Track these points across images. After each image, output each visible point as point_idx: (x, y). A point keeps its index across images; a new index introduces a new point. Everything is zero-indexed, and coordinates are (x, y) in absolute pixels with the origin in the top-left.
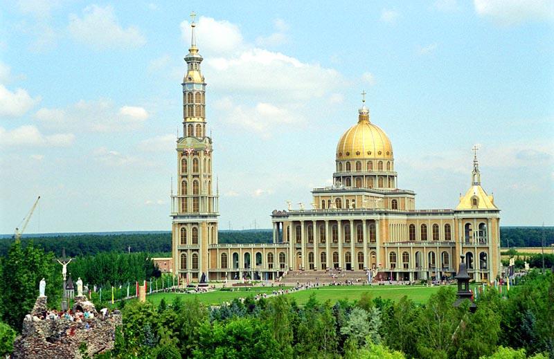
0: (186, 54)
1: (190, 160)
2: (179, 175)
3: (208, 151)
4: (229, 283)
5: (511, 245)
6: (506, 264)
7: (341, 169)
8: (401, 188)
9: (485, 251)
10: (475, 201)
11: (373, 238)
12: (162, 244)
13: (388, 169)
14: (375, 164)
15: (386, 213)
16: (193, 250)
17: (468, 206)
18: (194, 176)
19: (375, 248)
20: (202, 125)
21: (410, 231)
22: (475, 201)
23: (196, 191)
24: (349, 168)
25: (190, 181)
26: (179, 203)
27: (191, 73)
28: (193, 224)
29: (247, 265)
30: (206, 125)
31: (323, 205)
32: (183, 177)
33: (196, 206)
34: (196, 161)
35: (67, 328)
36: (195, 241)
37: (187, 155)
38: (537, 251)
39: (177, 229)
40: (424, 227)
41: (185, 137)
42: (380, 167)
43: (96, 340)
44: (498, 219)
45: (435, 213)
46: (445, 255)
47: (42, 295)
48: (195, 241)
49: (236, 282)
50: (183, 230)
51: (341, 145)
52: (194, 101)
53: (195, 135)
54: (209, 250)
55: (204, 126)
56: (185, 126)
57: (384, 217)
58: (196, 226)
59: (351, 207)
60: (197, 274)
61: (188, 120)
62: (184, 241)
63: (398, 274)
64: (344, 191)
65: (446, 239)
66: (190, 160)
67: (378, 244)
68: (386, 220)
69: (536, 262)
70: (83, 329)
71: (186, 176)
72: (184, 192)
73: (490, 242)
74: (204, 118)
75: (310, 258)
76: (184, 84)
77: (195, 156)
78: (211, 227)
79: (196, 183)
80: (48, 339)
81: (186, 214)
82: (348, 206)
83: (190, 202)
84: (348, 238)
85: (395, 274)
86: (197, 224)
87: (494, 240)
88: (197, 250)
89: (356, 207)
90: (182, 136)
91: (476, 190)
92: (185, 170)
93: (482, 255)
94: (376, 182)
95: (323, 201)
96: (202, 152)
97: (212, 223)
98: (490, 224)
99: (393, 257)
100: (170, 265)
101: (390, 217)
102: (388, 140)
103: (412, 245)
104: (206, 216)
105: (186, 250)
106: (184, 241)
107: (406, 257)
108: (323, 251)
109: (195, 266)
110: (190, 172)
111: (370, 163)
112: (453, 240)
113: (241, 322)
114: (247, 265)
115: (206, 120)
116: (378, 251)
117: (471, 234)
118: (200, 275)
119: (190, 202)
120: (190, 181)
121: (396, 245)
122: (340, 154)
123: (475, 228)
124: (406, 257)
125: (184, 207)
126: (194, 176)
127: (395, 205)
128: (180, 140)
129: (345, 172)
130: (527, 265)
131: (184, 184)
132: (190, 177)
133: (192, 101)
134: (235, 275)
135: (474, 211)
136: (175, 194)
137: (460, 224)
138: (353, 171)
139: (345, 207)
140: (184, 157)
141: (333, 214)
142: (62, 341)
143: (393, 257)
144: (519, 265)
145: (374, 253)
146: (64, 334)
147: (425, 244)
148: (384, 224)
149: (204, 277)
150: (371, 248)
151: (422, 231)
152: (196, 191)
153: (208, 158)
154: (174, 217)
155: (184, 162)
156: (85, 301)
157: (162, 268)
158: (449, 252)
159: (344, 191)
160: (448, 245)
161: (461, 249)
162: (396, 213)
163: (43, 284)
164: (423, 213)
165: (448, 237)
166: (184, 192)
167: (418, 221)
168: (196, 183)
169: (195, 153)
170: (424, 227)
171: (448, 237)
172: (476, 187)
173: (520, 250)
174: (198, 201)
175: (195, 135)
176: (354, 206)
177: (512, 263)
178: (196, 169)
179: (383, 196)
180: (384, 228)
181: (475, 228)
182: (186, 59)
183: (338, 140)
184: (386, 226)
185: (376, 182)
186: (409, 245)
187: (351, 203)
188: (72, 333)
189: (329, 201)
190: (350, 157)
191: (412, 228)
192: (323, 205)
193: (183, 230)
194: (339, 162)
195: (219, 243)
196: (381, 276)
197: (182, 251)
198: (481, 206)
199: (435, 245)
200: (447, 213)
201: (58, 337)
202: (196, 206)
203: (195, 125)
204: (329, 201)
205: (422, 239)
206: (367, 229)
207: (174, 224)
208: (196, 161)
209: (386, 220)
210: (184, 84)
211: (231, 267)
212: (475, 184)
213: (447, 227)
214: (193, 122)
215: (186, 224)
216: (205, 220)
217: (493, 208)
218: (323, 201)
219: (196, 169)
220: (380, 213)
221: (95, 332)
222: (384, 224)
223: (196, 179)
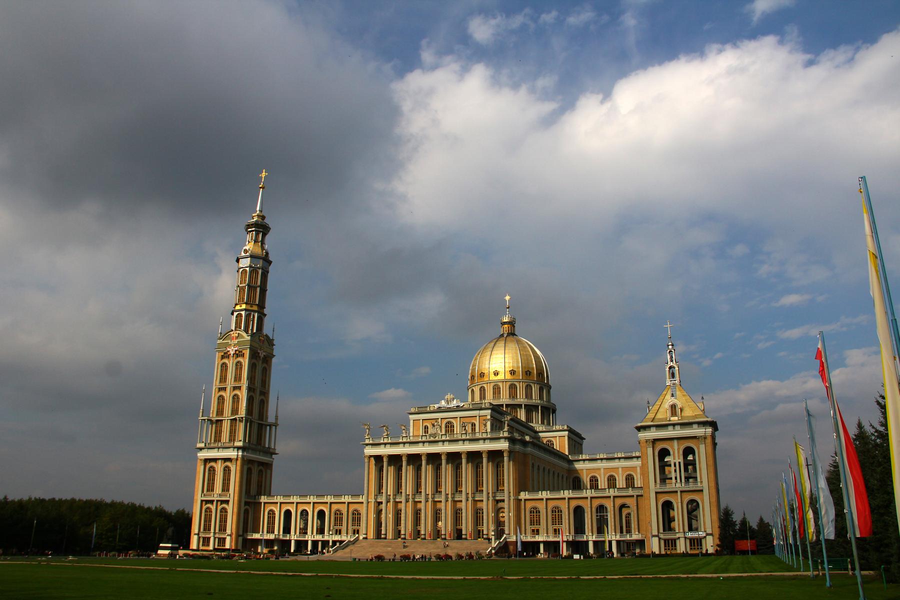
25: (228, 395)
36: (226, 488)
48: (226, 488)
62: (211, 488)
63: (542, 546)
72: (220, 412)
79: (236, 399)
97: (261, 464)
126: (235, 388)
140: (225, 360)
158: (631, 502)
161: (653, 495)
166: (220, 412)
193: (212, 470)
197: (207, 502)
214: (242, 310)
215: (215, 460)
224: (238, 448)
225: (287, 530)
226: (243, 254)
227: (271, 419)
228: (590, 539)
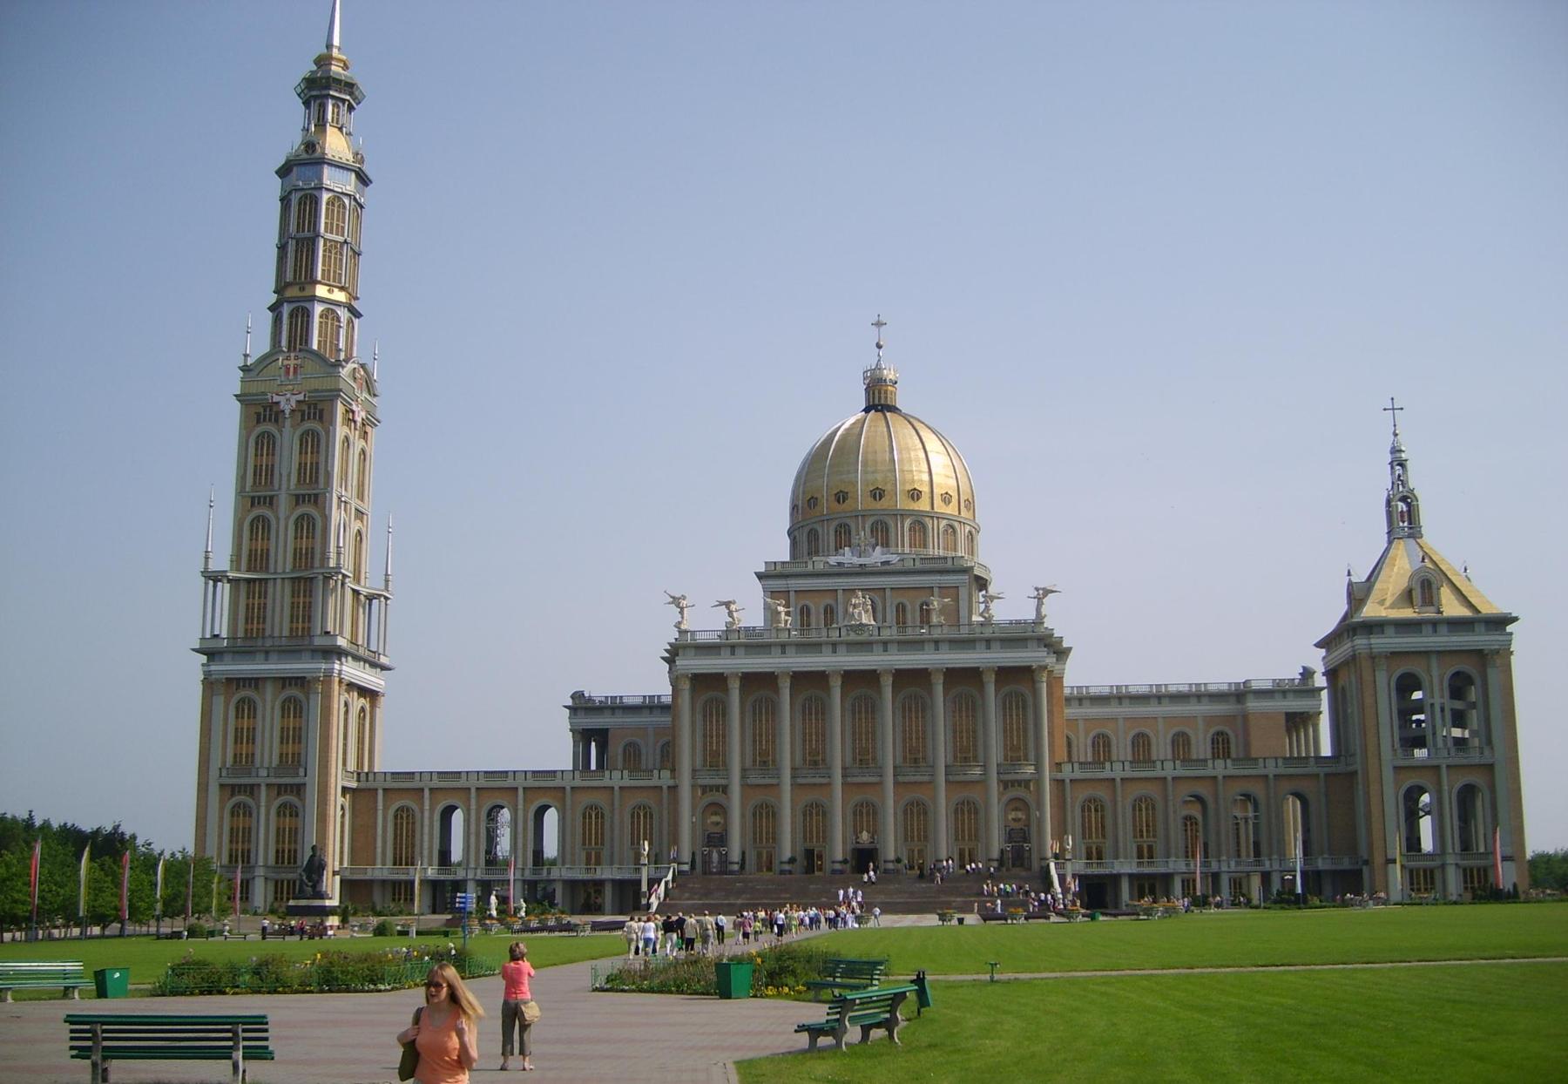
2: (241, 491)
16: (281, 789)
18: (299, 499)
28: (285, 681)
32: (255, 501)
39: (219, 702)
50: (246, 708)
54: (344, 789)
77: (308, 425)
78: (358, 703)
83: (280, 600)
86: (301, 682)
105: (251, 790)
119: (280, 600)
132: (283, 503)
137: (1381, 678)
141: (865, 646)
154: (212, 654)
174: (310, 593)
193: (246, 708)
207: (209, 684)
215: (255, 682)
226: (305, 156)
228: (1224, 868)
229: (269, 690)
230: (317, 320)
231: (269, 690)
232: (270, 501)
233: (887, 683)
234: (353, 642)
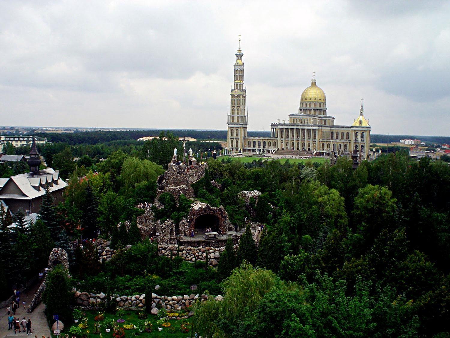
0: (236, 52)
1: (236, 99)
3: (244, 95)
4: (251, 154)
5: (374, 142)
6: (371, 150)
7: (302, 106)
8: (328, 115)
9: (363, 144)
10: (361, 122)
11: (315, 137)
12: (223, 135)
13: (323, 106)
14: (308, 104)
15: (321, 126)
16: (236, 139)
17: (358, 125)
18: (238, 107)
19: (315, 141)
20: (242, 84)
21: (331, 135)
22: (361, 122)
23: (238, 113)
24: (306, 106)
25: (236, 108)
26: (231, 119)
27: (238, 61)
28: (236, 127)
29: (259, 146)
30: (244, 84)
31: (294, 121)
32: (233, 107)
33: (238, 120)
34: (238, 100)
35: (186, 169)
36: (237, 135)
37: (235, 97)
38: (386, 145)
40: (337, 133)
41: (234, 89)
42: (320, 106)
43: (197, 175)
44: (370, 131)
45: (343, 127)
46: (346, 146)
47: (175, 155)
48: (237, 135)
49: (254, 153)
51: (302, 95)
52: (239, 73)
53: (239, 88)
55: (243, 85)
56: (234, 84)
57: (320, 128)
58: (238, 129)
59: (306, 123)
60: (238, 149)
61: (236, 82)
62: (232, 135)
64: (303, 116)
65: (347, 139)
66: (236, 99)
67: (317, 140)
68: (321, 129)
69: (384, 150)
70: (192, 169)
71: (239, 107)
72: (233, 113)
73: (366, 140)
74: (243, 81)
75: (287, 144)
76: (235, 66)
77: (238, 98)
78: (244, 129)
79: (238, 110)
80: (178, 173)
81: (233, 123)
82: (305, 123)
83: (236, 118)
84: (304, 136)
85: (323, 153)
86: (238, 127)
87: (367, 140)
88: (238, 139)
89: (308, 123)
90: (233, 89)
91: (361, 118)
92: (234, 104)
93: (362, 146)
94: (318, 112)
95: (294, 120)
96: (242, 96)
97: (245, 128)
98: (366, 133)
99: (323, 146)
100: (226, 144)
101: (323, 128)
102: (323, 93)
103: (332, 140)
104: (242, 125)
105: (233, 139)
106: (232, 135)
107: (329, 146)
108: (293, 142)
109: (237, 146)
110: (236, 105)
111: (315, 104)
112: (349, 139)
113: (255, 169)
114: (259, 146)
115: (244, 82)
116: (317, 143)
117: (358, 137)
118: (239, 150)
119: (236, 118)
120: (236, 108)
121: (325, 140)
122: (302, 99)
123: (360, 134)
124: (329, 146)
125: (233, 120)
126: (238, 107)
127: (325, 123)
128: (232, 91)
129: (304, 107)
130: (380, 151)
131: (233, 110)
132: (236, 107)
133: (239, 74)
134: (254, 150)
135: (360, 127)
136: (229, 114)
138: (308, 107)
139: (303, 123)
140: (234, 98)
142: (183, 174)
143: (323, 146)
144: (377, 151)
145: (315, 143)
146: (184, 171)
147: (337, 141)
148: (320, 131)
149: (240, 150)
150: (314, 141)
151: (336, 135)
152: (238, 113)
153: (244, 99)
154: (229, 124)
155: (233, 100)
156: (192, 158)
157: (223, 146)
158: (348, 144)
159: (303, 116)
160: (348, 141)
162: (325, 126)
163: (176, 150)
164: (338, 127)
165: (347, 138)
166: (233, 113)
167: (335, 130)
168: (238, 110)
169: (239, 96)
170: (337, 133)
171: (347, 138)
172: (361, 116)
173: (378, 145)
174: (239, 117)
175: (239, 88)
176: (307, 122)
177: (374, 150)
178: (239, 104)
179: (320, 118)
180: (320, 133)
181: (360, 134)
182: (236, 55)
183: (302, 93)
184: (321, 132)
185: (318, 112)
186: (330, 141)
187: (306, 121)
188: (188, 171)
189: (296, 120)
190: (307, 101)
191: (332, 133)
192: (294, 121)
193: (232, 130)
194: (302, 103)
195: (247, 136)
196: (317, 154)
197: (231, 139)
198: (363, 125)
199: (342, 141)
200: (348, 127)
201: (182, 172)
202: (238, 120)
203: (239, 84)
204: (296, 120)
205: (336, 138)
206: (313, 134)
208: (238, 100)
209: (321, 129)
210: (235, 66)
211: (252, 147)
212: (361, 115)
213: (348, 133)
215: (233, 127)
216: (242, 126)
217: (368, 126)
218: (294, 120)
219: (239, 104)
220: (319, 126)
221: (197, 171)
222: (320, 131)
223: (239, 108)
224: (241, 125)
225: (254, 146)
226: (237, 65)
227: (246, 115)
229: (235, 128)
230: (239, 85)
231: (235, 128)
232: (234, 107)
233: (300, 130)
234: (244, 122)
